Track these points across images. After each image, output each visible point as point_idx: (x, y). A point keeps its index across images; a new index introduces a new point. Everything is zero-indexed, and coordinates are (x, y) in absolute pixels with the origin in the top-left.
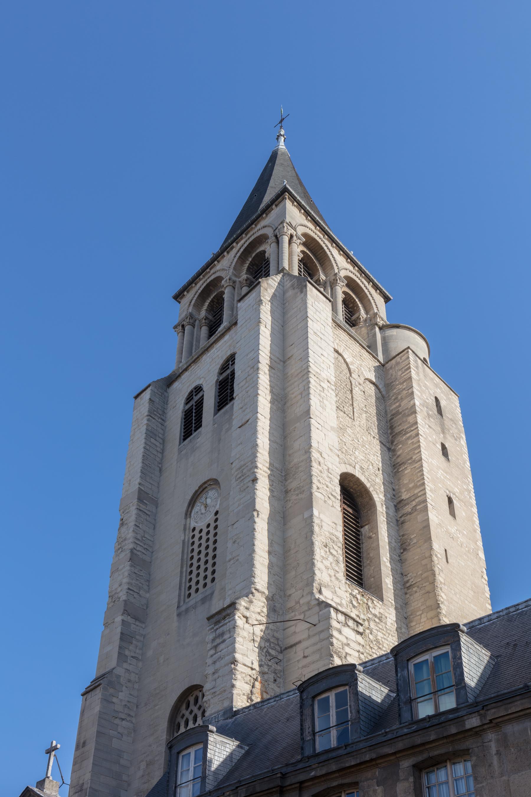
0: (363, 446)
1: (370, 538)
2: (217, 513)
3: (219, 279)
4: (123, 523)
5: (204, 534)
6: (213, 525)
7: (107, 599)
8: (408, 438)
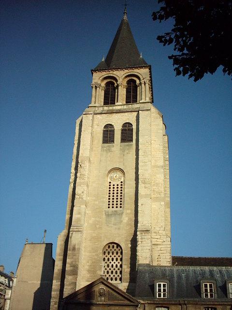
5: (116, 187)
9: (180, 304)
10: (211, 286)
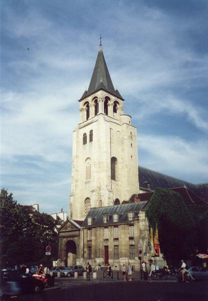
9: (95, 227)
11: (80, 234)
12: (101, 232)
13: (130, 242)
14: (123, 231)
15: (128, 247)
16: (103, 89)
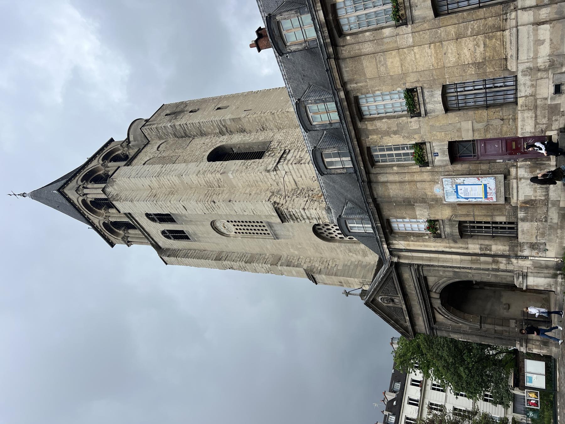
0: (193, 151)
1: (239, 148)
2: (228, 221)
3: (104, 224)
4: (232, 268)
5: (238, 228)
6: (234, 223)
7: (269, 274)
8: (188, 129)
10: (329, 156)
11: (410, 265)
12: (391, 178)
13: (417, 13)
14: (369, 67)
15: (449, 26)
16: (63, 187)
